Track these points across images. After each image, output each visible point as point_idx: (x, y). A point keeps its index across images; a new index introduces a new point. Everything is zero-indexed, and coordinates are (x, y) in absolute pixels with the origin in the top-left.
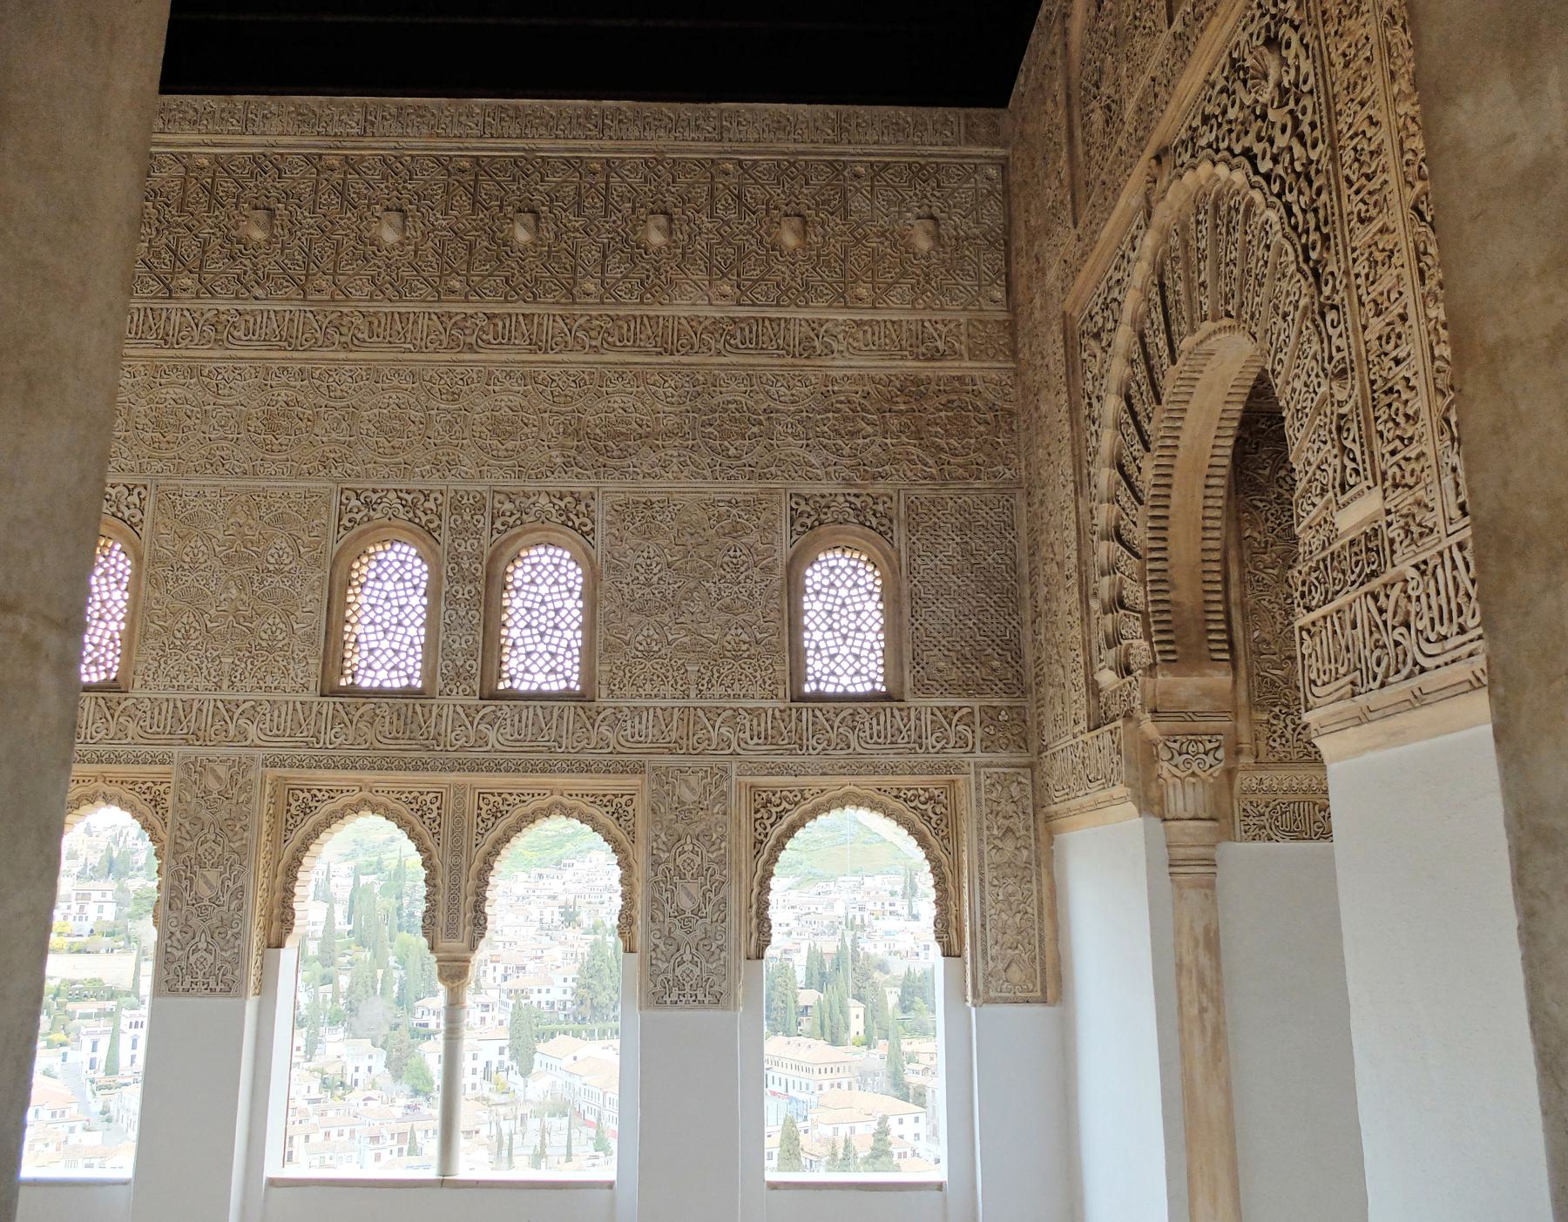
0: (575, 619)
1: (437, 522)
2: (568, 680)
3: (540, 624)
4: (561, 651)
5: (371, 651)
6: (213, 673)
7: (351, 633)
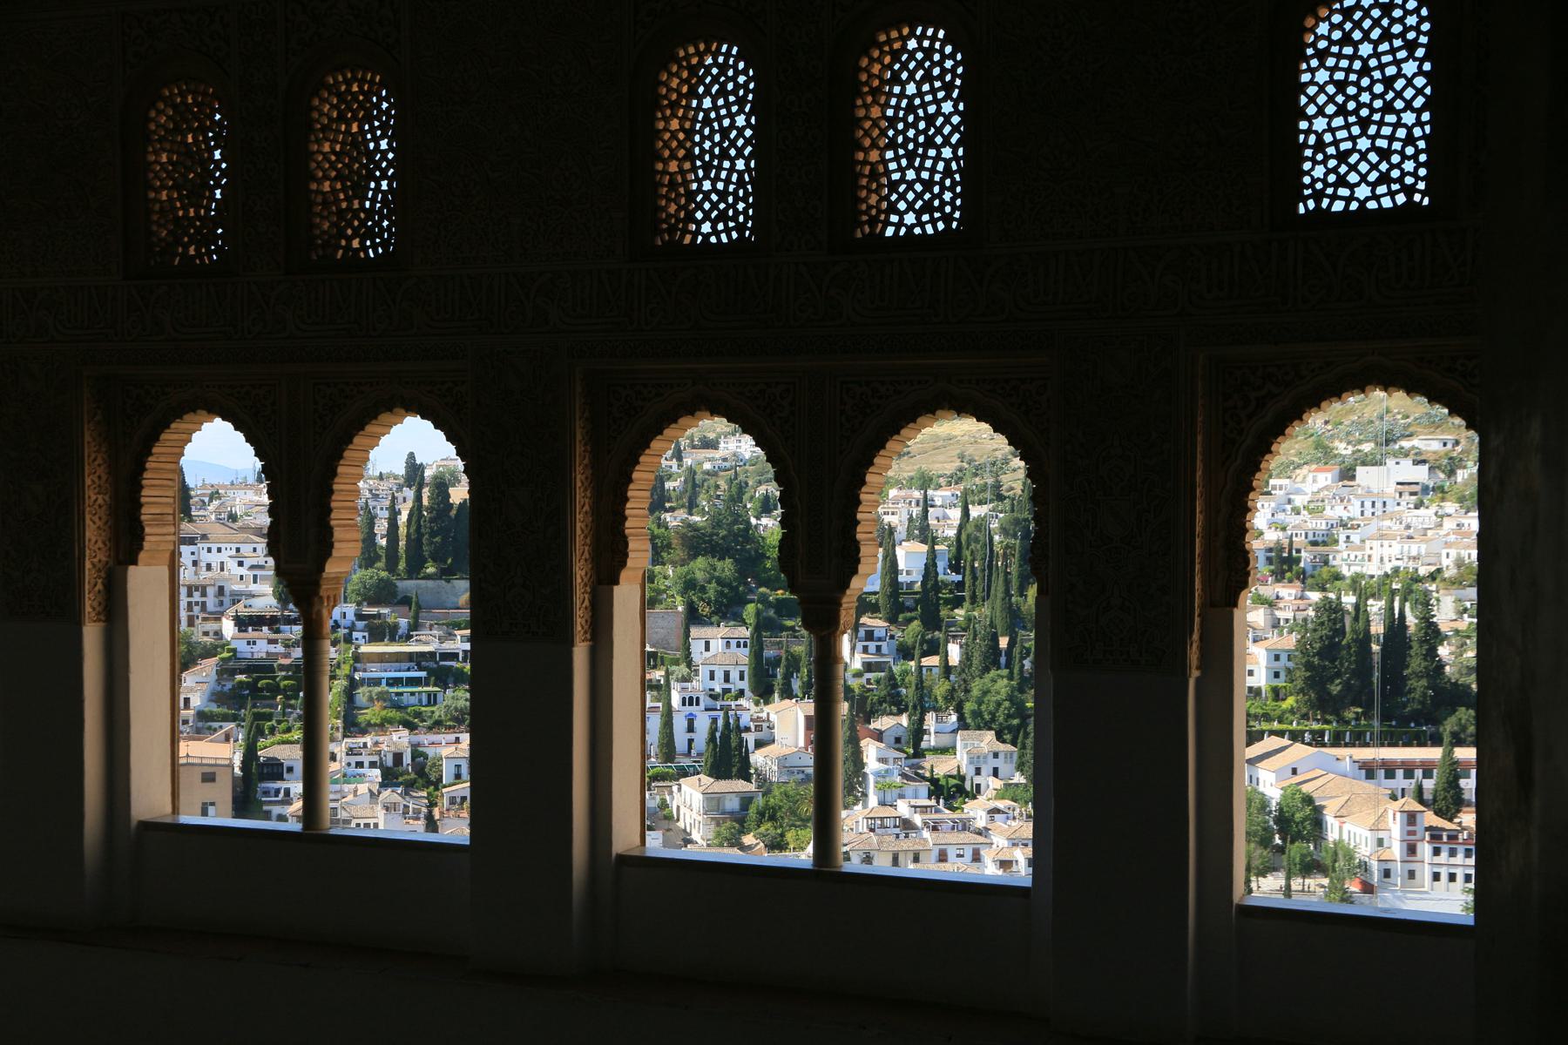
0: (1420, 92)
2: (1409, 191)
3: (1360, 106)
4: (1397, 146)
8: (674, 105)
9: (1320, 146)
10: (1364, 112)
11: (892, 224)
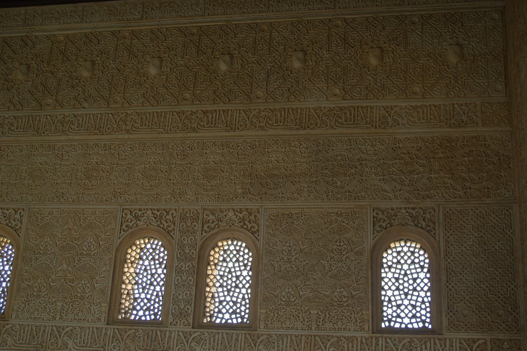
1: (257, 228)
2: (424, 322)
4: (418, 304)
5: (221, 302)
6: (307, 320)
7: (385, 296)
8: (132, 263)
9: (390, 301)
10: (406, 290)
11: (219, 318)
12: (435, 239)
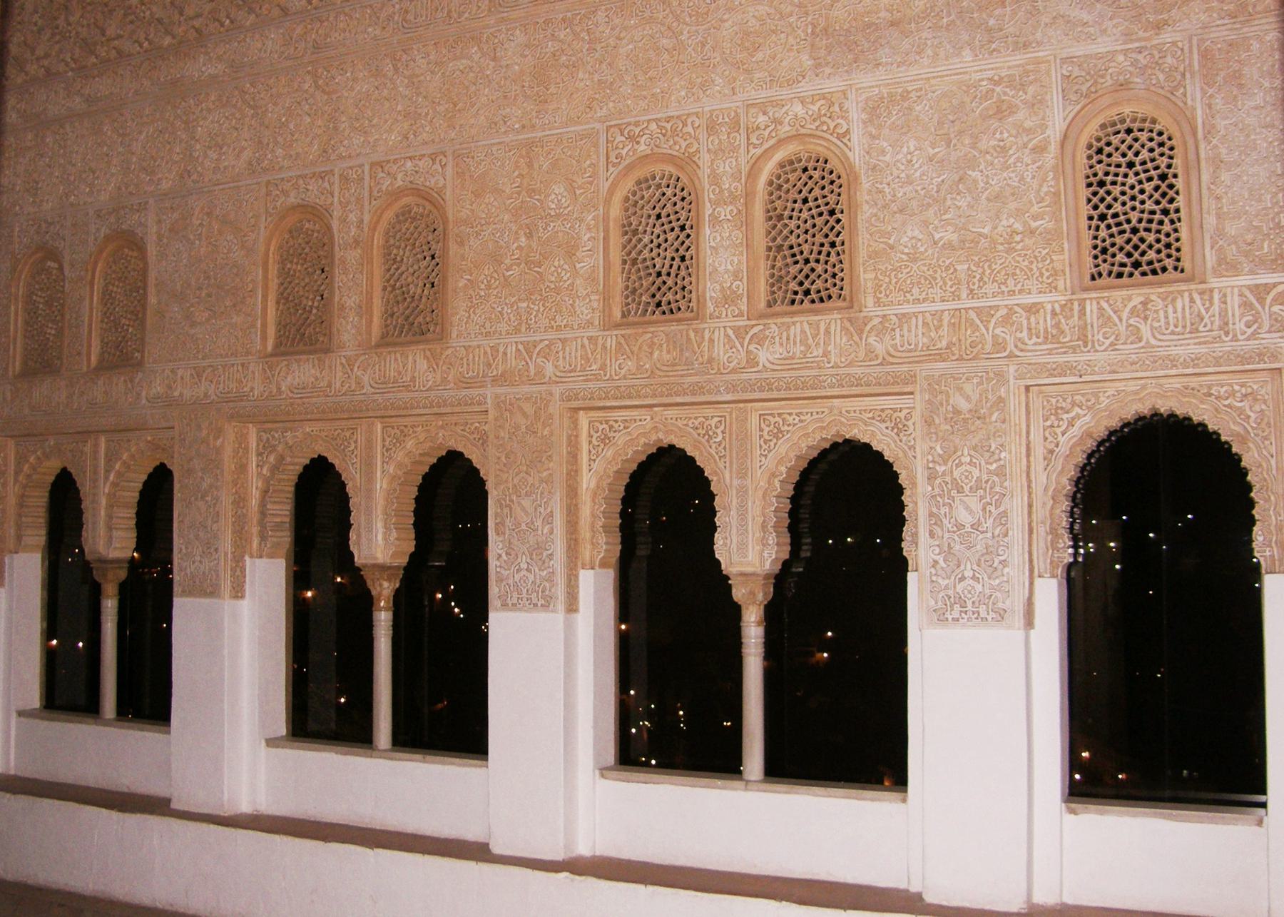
12: (1185, 103)
